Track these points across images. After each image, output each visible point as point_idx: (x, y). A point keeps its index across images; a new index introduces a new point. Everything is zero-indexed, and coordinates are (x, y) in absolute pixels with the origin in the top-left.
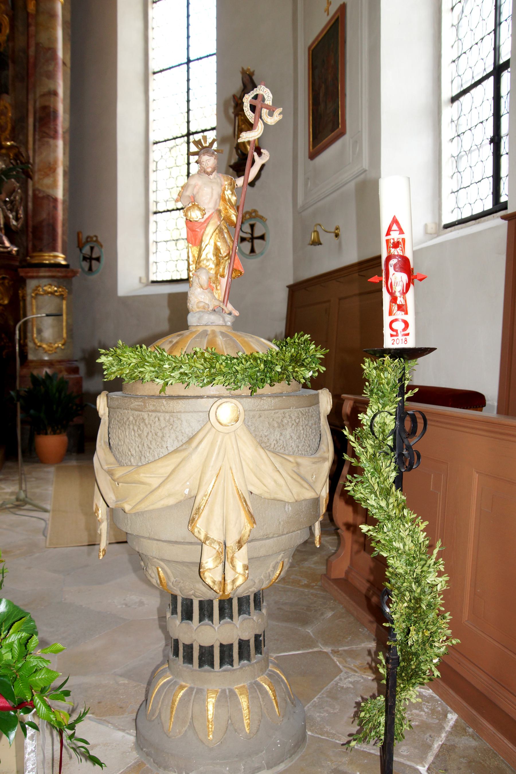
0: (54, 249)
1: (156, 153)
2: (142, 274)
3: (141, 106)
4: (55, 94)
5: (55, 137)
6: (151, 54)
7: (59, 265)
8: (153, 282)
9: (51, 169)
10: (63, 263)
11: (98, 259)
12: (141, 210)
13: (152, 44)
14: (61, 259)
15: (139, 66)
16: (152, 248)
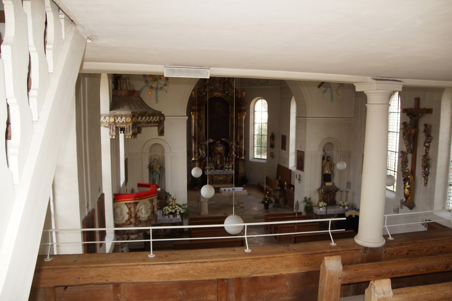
0: (242, 156)
1: (256, 136)
2: (253, 157)
3: (253, 129)
4: (243, 133)
5: (243, 140)
6: (255, 120)
7: (243, 159)
8: (255, 158)
9: (243, 145)
10: (244, 158)
11: (246, 154)
12: (253, 146)
13: (255, 118)
14: (243, 158)
15: (253, 122)
16: (254, 152)
